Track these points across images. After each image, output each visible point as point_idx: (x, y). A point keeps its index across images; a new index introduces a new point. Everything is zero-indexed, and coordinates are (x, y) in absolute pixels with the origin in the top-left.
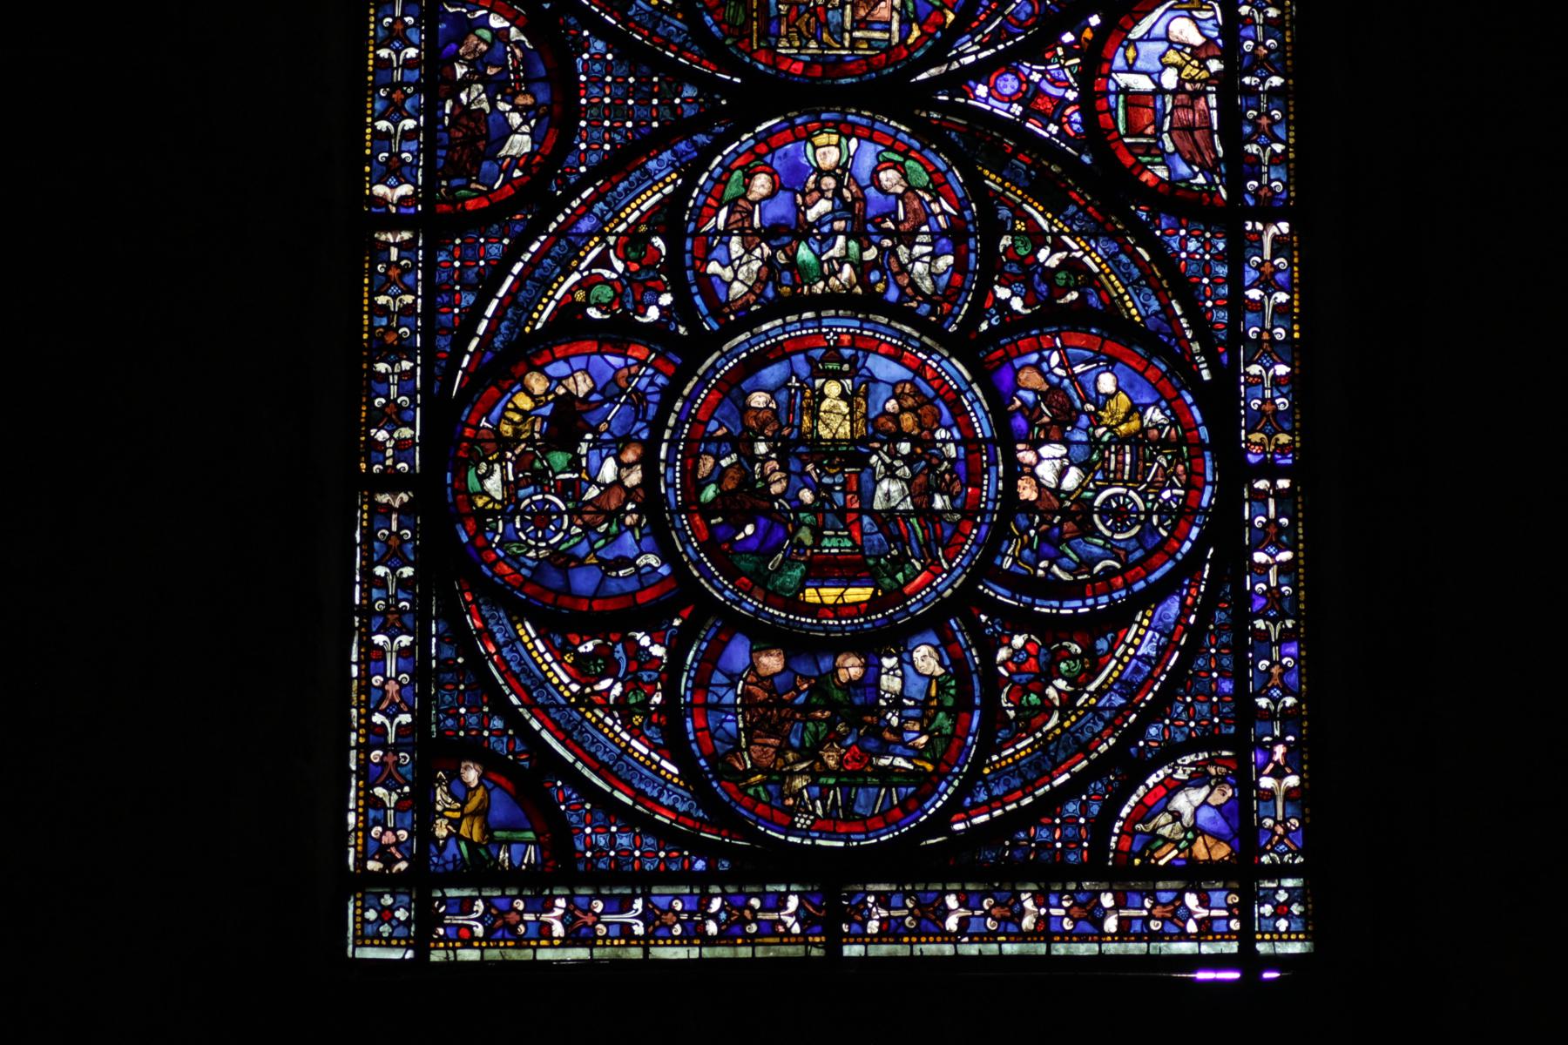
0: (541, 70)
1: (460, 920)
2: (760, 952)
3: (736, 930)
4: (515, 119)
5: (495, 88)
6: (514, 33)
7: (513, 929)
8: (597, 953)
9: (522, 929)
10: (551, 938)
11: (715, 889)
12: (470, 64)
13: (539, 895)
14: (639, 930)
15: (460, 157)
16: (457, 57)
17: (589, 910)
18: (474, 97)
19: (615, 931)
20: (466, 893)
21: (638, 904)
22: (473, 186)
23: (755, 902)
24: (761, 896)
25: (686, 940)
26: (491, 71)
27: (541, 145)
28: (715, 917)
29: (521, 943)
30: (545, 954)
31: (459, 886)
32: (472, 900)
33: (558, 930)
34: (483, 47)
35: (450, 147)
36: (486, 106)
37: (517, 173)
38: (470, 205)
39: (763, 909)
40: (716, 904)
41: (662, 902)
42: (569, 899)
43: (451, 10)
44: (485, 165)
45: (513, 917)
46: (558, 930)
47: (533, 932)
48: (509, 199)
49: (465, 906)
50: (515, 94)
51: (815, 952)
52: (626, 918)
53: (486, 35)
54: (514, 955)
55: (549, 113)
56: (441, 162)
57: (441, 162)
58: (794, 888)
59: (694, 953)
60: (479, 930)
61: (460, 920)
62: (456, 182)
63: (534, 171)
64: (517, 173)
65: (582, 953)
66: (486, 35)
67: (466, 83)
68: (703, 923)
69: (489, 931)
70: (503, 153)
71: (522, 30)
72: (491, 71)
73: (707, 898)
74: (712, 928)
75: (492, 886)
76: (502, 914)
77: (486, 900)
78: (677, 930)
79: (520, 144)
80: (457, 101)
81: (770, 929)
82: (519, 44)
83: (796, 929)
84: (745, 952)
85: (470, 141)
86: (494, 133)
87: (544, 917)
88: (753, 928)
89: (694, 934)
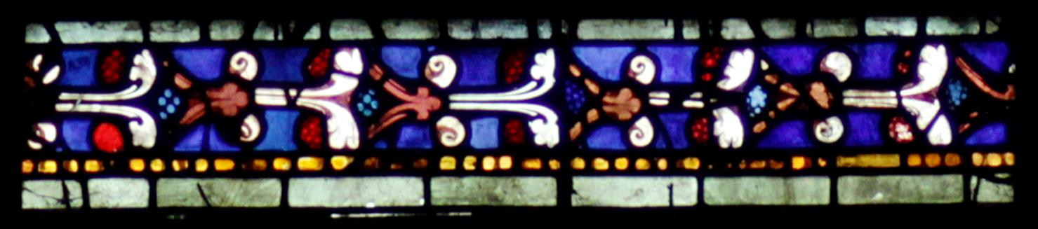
1: (96, 103)
2: (851, 192)
3: (791, 134)
7: (230, 127)
8: (442, 190)
9: (251, 127)
10: (325, 152)
11: (737, 29)
13: (294, 40)
14: (546, 132)
17: (420, 81)
19: (486, 134)
20: (112, 33)
21: (545, 66)
23: (839, 64)
24: (855, 47)
25: (665, 157)
28: (737, 100)
29: (249, 163)
30: (310, 194)
31: (93, 17)
32: (127, 51)
33: (344, 131)
39: (858, 81)
40: (739, 68)
41: (604, 62)
42: (371, 51)
45: (229, 98)
46: (344, 131)
47: (279, 136)
49: (109, 68)
51: (989, 193)
52: (513, 100)
54: (233, 194)
58: (936, 27)
59: (685, 193)
60: (145, 132)
61: (96, 103)
65: (403, 191)
68: (707, 117)
69: (169, 133)
73: (715, 52)
74: (729, 129)
75: (176, 17)
76: (201, 89)
77: (162, 52)
78: (643, 134)
81: (873, 133)
83: (941, 134)
84: (812, 191)
87: (309, 98)
88: (832, 131)
89: (684, 144)
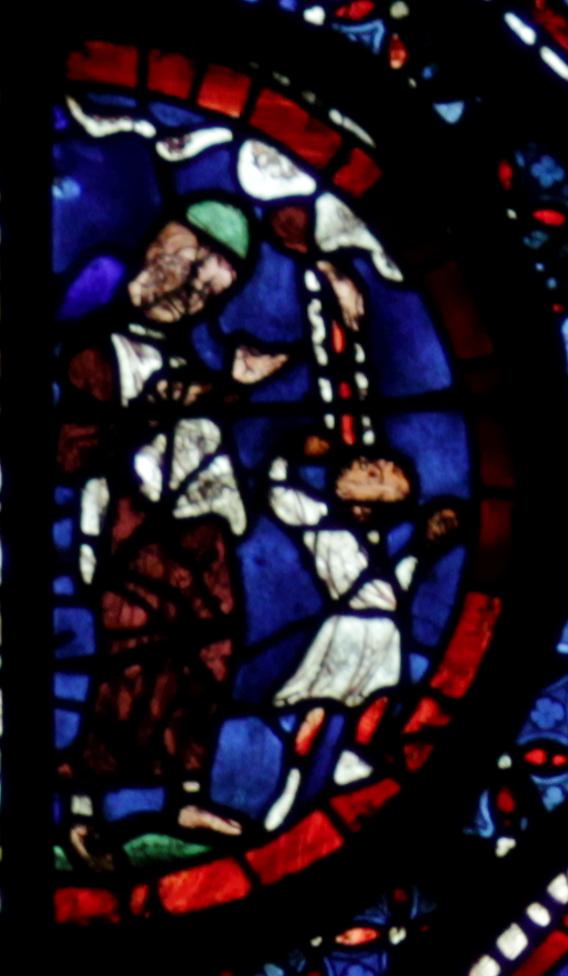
0: (434, 366)
4: (341, 557)
5: (262, 432)
6: (334, 224)
12: (170, 341)
15: (140, 705)
16: (122, 314)
18: (190, 466)
22: (189, 817)
26: (250, 369)
27: (436, 658)
34: (217, 274)
35: (101, 668)
36: (230, 505)
37: (350, 769)
38: (180, 891)
43: (97, 128)
44: (233, 737)
48: (322, 867)
50: (341, 458)
53: (228, 224)
55: (463, 534)
56: (68, 725)
57: (68, 725)
62: (126, 802)
63: (415, 758)
64: (350, 769)
66: (228, 224)
67: (156, 415)
70: (294, 690)
71: (362, 208)
72: (250, 369)
79: (357, 655)
80: (125, 485)
82: (349, 261)
85: (176, 636)
86: (264, 611)
